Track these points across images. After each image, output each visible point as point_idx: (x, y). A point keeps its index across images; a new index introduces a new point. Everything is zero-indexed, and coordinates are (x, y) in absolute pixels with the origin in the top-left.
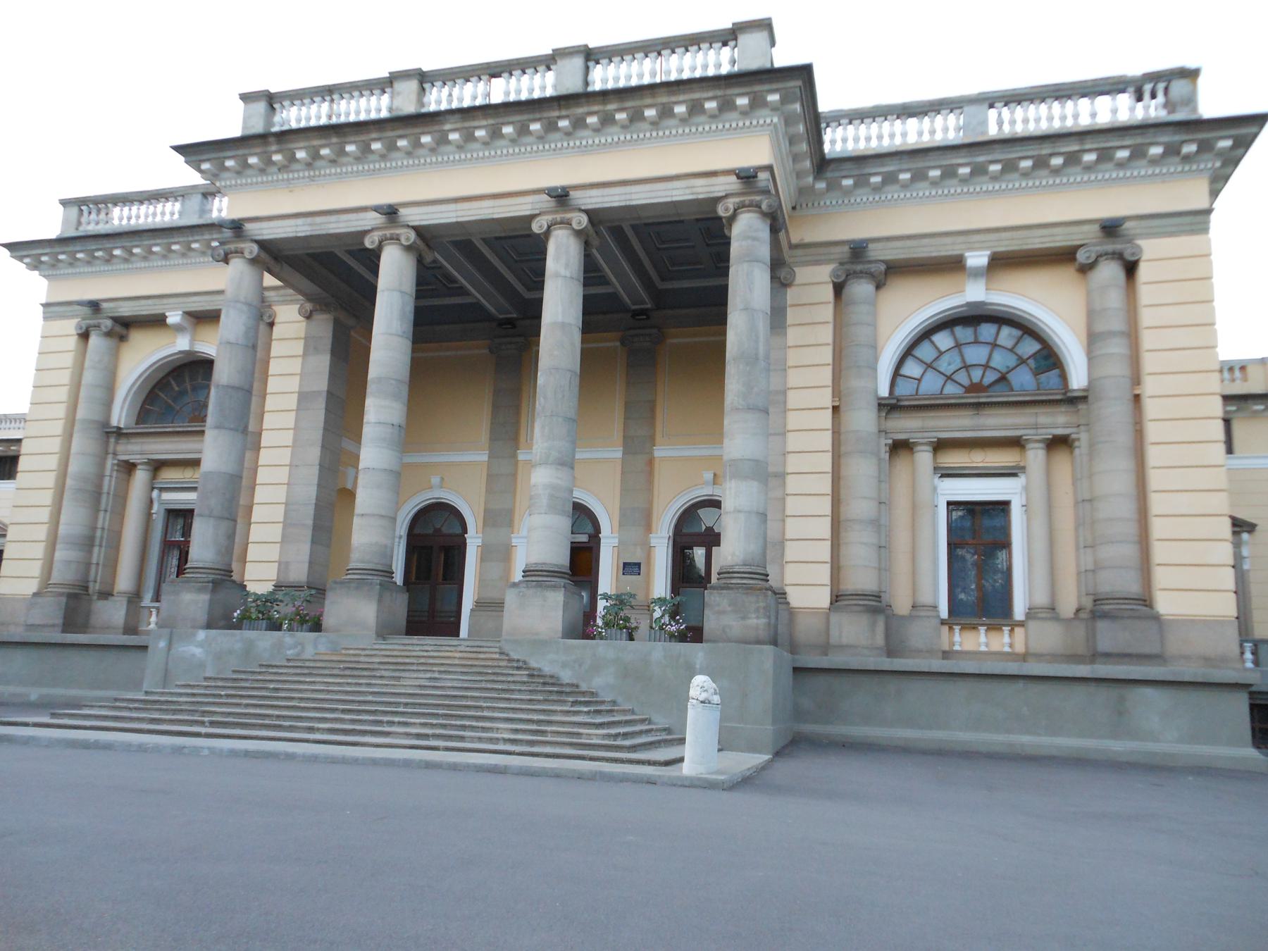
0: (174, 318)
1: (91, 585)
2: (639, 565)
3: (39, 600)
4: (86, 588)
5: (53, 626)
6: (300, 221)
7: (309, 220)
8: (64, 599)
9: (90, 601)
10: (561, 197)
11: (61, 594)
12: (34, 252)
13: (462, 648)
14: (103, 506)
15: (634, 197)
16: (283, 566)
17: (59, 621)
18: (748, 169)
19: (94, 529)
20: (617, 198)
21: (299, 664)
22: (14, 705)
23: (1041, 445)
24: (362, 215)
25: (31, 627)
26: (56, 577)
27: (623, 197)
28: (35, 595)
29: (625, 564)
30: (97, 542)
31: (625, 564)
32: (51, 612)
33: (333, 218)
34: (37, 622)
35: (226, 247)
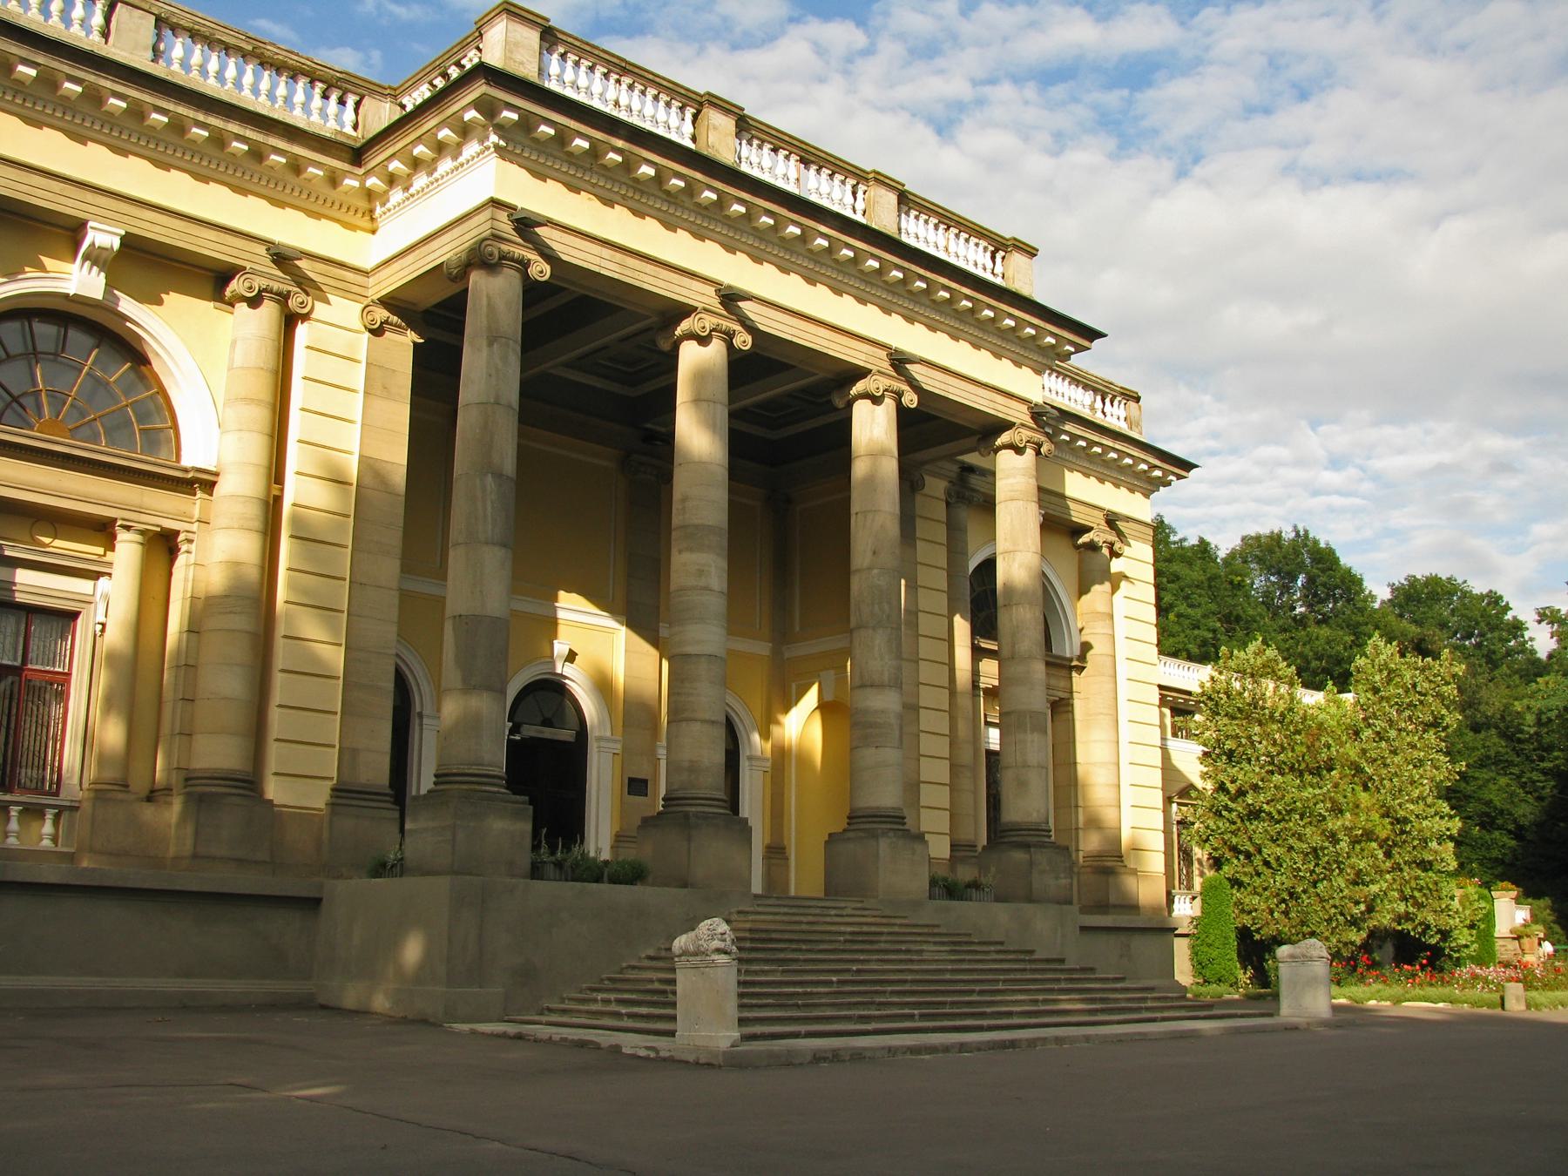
0: (102, 236)
2: (645, 782)
6: (607, 253)
7: (618, 256)
10: (899, 362)
12: (182, 110)
13: (849, 911)
15: (951, 390)
16: (348, 755)
18: (902, 352)
20: (937, 384)
21: (764, 935)
22: (332, 1008)
23: (139, 538)
24: (686, 281)
27: (943, 387)
29: (631, 780)
31: (631, 780)
33: (649, 268)
35: (505, 247)
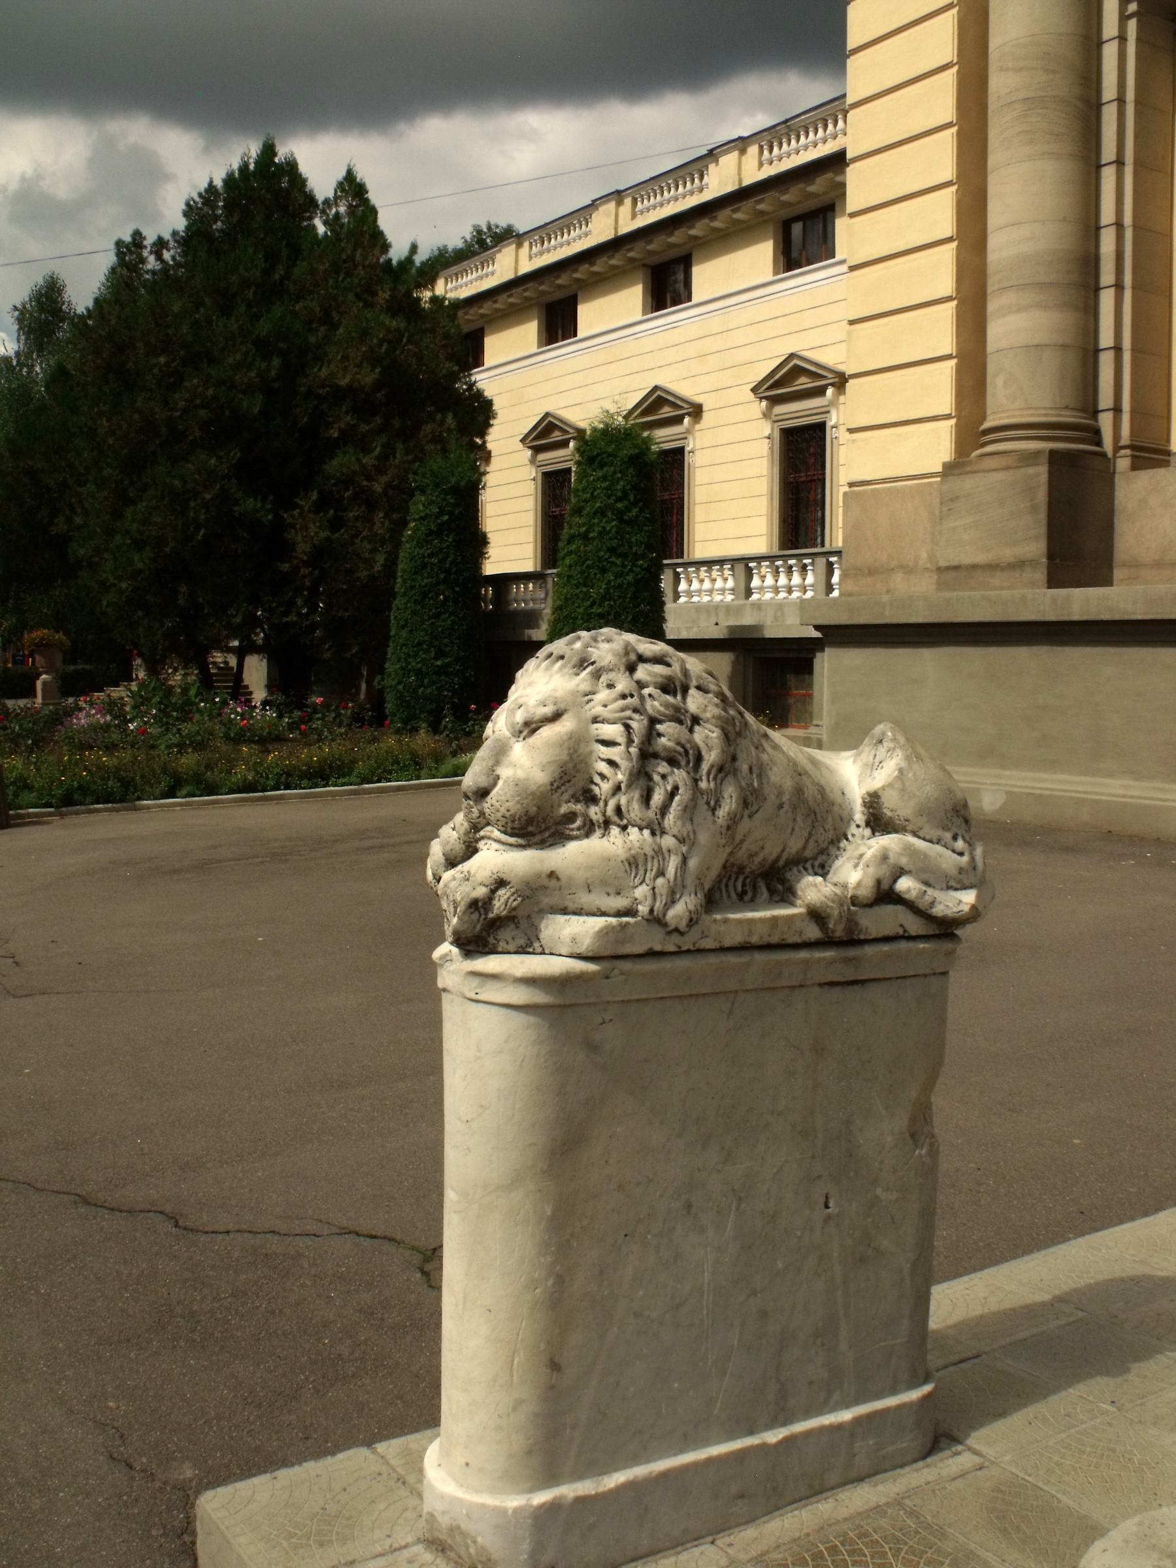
1: (1105, 422)
3: (966, 484)
4: (1095, 435)
5: (1018, 565)
8: (1040, 473)
9: (1108, 477)
11: (1029, 458)
14: (1108, 152)
17: (1036, 548)
19: (1089, 227)
25: (952, 574)
26: (1006, 402)
28: (949, 469)
30: (1107, 276)
32: (1004, 522)
34: (968, 557)
